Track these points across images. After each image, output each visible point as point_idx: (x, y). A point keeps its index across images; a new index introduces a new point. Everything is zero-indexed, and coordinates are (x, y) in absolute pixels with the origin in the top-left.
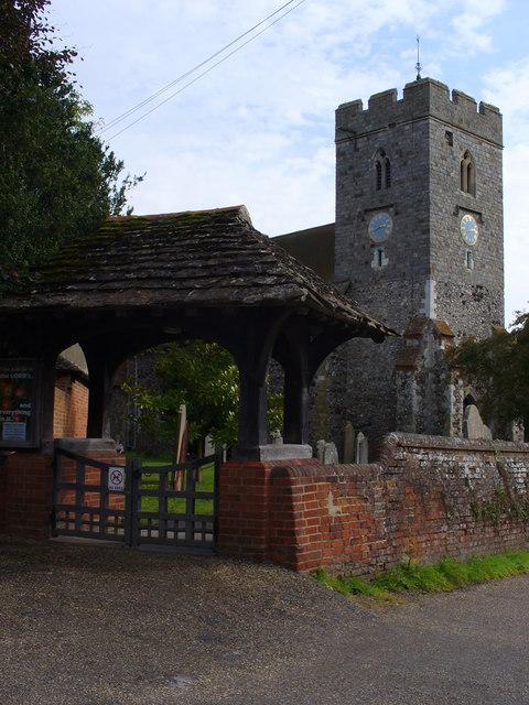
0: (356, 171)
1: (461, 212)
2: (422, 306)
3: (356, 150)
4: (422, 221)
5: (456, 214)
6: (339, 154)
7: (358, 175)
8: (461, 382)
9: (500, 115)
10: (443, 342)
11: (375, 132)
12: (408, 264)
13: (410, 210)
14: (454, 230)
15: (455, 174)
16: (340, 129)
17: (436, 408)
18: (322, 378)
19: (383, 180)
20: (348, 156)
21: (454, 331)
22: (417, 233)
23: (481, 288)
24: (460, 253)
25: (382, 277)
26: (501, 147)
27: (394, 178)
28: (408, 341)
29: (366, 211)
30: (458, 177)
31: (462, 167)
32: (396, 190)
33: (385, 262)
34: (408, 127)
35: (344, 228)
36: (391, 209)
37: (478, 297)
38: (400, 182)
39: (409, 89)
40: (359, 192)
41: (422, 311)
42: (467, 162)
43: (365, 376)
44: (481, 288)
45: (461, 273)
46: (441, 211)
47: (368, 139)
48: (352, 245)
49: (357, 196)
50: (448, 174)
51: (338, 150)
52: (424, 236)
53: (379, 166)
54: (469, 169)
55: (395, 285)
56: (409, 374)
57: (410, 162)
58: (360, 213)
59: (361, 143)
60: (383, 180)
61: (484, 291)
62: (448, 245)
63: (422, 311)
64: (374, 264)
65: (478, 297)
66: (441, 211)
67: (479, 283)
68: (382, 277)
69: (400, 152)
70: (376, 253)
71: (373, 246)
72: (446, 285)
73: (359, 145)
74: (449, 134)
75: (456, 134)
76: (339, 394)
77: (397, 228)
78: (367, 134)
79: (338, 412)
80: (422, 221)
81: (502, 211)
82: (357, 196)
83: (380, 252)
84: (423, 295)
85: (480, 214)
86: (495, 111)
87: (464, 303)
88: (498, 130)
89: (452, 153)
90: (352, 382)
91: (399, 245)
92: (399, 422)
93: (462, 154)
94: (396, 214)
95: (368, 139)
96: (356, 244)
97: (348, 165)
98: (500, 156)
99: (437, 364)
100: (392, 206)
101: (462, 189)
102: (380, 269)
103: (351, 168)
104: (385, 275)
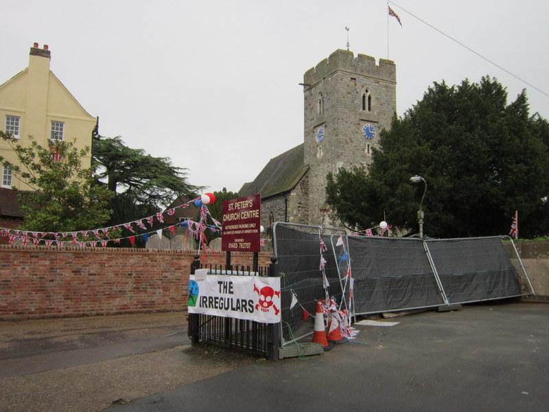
0: (311, 107)
1: (362, 123)
3: (311, 95)
5: (359, 124)
6: (306, 98)
9: (394, 65)
11: (317, 83)
14: (357, 133)
15: (359, 102)
24: (362, 145)
27: (325, 107)
29: (315, 127)
31: (364, 97)
34: (330, 79)
36: (324, 125)
38: (327, 109)
39: (331, 57)
42: (368, 94)
43: (315, 216)
50: (353, 102)
51: (305, 96)
52: (336, 138)
53: (320, 103)
54: (369, 98)
55: (326, 165)
56: (325, 213)
62: (352, 142)
64: (318, 156)
68: (321, 162)
71: (317, 146)
72: (351, 164)
74: (352, 79)
75: (359, 79)
89: (356, 90)
93: (364, 89)
94: (326, 126)
98: (394, 88)
101: (364, 108)
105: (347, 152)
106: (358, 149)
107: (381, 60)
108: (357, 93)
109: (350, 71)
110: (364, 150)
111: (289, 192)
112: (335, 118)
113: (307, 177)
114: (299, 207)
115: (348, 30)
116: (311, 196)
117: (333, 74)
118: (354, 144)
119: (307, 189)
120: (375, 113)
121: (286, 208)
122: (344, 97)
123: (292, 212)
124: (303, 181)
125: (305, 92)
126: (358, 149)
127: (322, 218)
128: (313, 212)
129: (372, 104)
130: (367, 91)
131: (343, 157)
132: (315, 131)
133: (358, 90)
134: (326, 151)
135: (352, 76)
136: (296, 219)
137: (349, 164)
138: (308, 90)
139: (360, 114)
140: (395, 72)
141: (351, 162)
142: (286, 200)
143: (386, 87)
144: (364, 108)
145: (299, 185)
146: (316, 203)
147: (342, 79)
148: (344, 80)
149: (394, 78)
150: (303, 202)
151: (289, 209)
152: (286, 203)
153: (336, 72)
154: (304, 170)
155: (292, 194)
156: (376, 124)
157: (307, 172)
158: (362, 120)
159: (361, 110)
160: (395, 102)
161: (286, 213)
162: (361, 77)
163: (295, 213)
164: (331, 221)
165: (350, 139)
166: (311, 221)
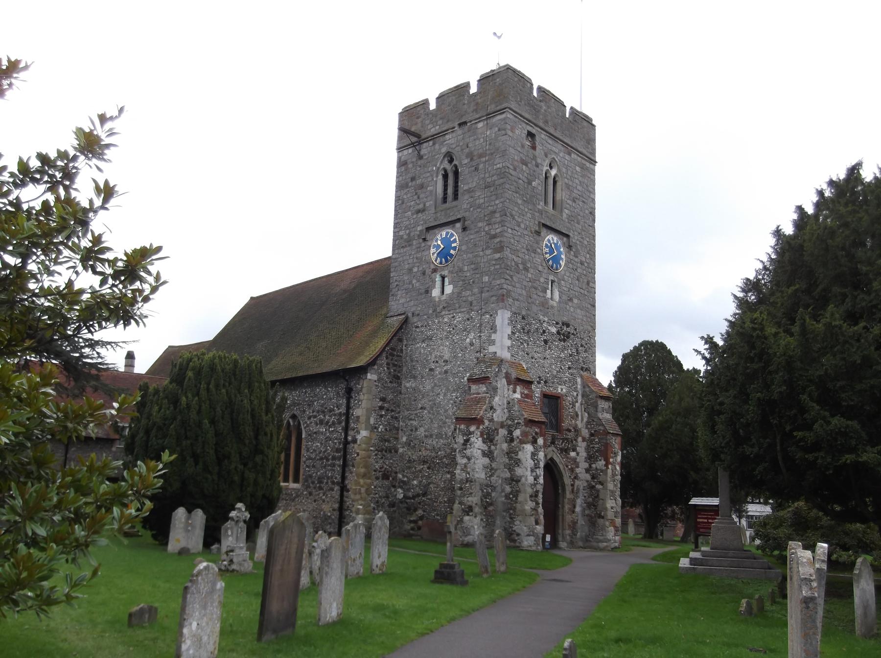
1: (544, 231)
2: (493, 342)
3: (420, 157)
4: (494, 237)
5: (538, 233)
6: (402, 164)
7: (422, 186)
8: (540, 441)
9: (594, 126)
10: (518, 389)
11: (442, 133)
12: (476, 290)
13: (480, 224)
14: (535, 252)
16: (404, 131)
17: (508, 475)
18: (364, 433)
19: (450, 190)
20: (410, 166)
21: (532, 376)
22: (488, 252)
23: (568, 325)
25: (444, 308)
26: (594, 162)
27: (463, 187)
28: (474, 387)
29: (428, 229)
30: (541, 188)
31: (546, 178)
32: (464, 201)
33: (449, 289)
34: (480, 125)
35: (402, 251)
36: (458, 225)
37: (564, 337)
38: (469, 191)
39: (484, 80)
40: (421, 206)
41: (492, 349)
42: (553, 172)
43: (421, 432)
44: (568, 325)
45: (544, 304)
46: (519, 226)
47: (434, 144)
48: (410, 270)
49: (418, 211)
50: (530, 183)
51: (399, 159)
52: (497, 256)
53: (445, 177)
54: (555, 182)
55: (459, 317)
56: (473, 428)
57: (481, 166)
58: (421, 231)
59: (425, 149)
60: (450, 190)
61: (570, 330)
62: (526, 269)
63: (492, 349)
64: (436, 293)
65: (564, 337)
66: (519, 226)
67: (565, 319)
69: (471, 156)
70: (438, 279)
71: (435, 271)
72: (523, 318)
73: (422, 153)
74: (530, 135)
75: (541, 137)
76: (389, 455)
77: (464, 248)
78: (433, 138)
79: (386, 476)
80: (494, 237)
81: (594, 236)
82: (418, 211)
83: (443, 278)
84: (494, 329)
85: (567, 236)
86: (587, 120)
87: (546, 342)
88: (591, 141)
89: (535, 158)
90: (404, 439)
91: (466, 268)
92: (459, 492)
93: (547, 162)
94: (464, 229)
95: (434, 144)
96: (415, 270)
97: (410, 175)
98: (593, 172)
99: (511, 418)
100: (458, 220)
101: (546, 203)
102: (444, 297)
103: (413, 179)
104: (449, 305)
105: (519, 291)
106: (536, 288)
107: (572, 108)
108: (537, 166)
109: (527, 116)
110: (544, 291)
111: (362, 371)
112: (495, 212)
113: (400, 340)
114: (381, 408)
115: (499, 37)
116: (408, 384)
117: (489, 115)
118: (530, 275)
119: (399, 367)
120: (565, 216)
121: (348, 407)
122: (515, 170)
123: (368, 419)
124: (393, 349)
125: (400, 149)
126: (536, 288)
127: (460, 439)
128: (415, 423)
129: (558, 197)
130: (551, 167)
131: (511, 300)
132: (428, 237)
133: (539, 161)
134: (463, 283)
135: (530, 129)
136: (374, 436)
137: (520, 317)
138: (413, 145)
139: (541, 212)
140: (594, 140)
141: (524, 313)
142: (349, 391)
143: (583, 167)
144: (546, 203)
145: (384, 355)
146: (424, 402)
147: (512, 130)
148: (517, 132)
149: (593, 152)
150: (390, 397)
151: (357, 412)
152: (349, 399)
153: (501, 111)
154: (395, 322)
155: (369, 376)
156: (565, 239)
157: (401, 328)
158: (545, 226)
159: (542, 203)
160: (593, 200)
161: (347, 422)
162: (543, 136)
163: (372, 421)
164: (485, 447)
165: (524, 263)
166: (408, 444)
